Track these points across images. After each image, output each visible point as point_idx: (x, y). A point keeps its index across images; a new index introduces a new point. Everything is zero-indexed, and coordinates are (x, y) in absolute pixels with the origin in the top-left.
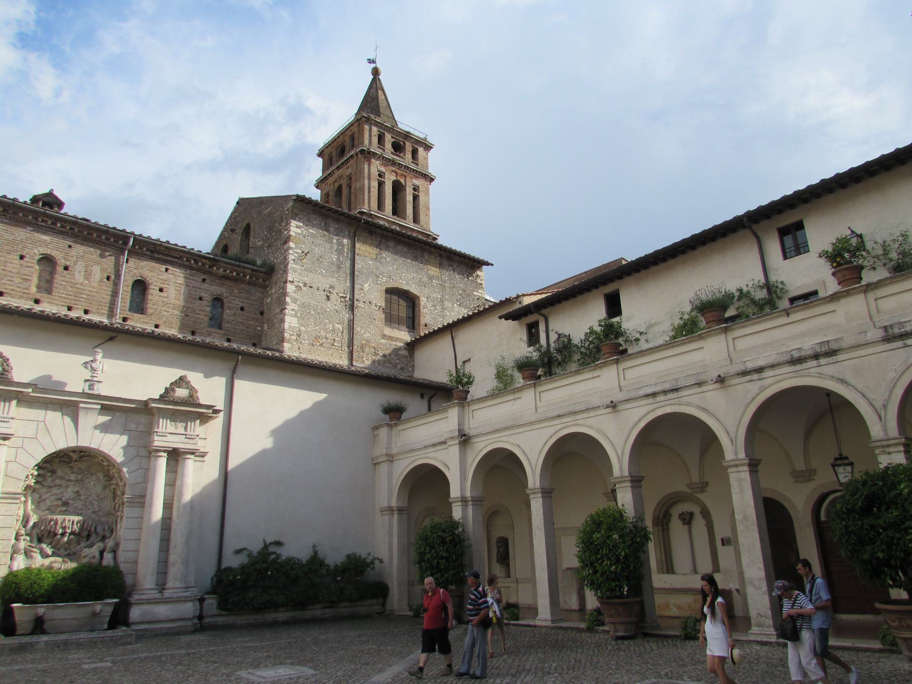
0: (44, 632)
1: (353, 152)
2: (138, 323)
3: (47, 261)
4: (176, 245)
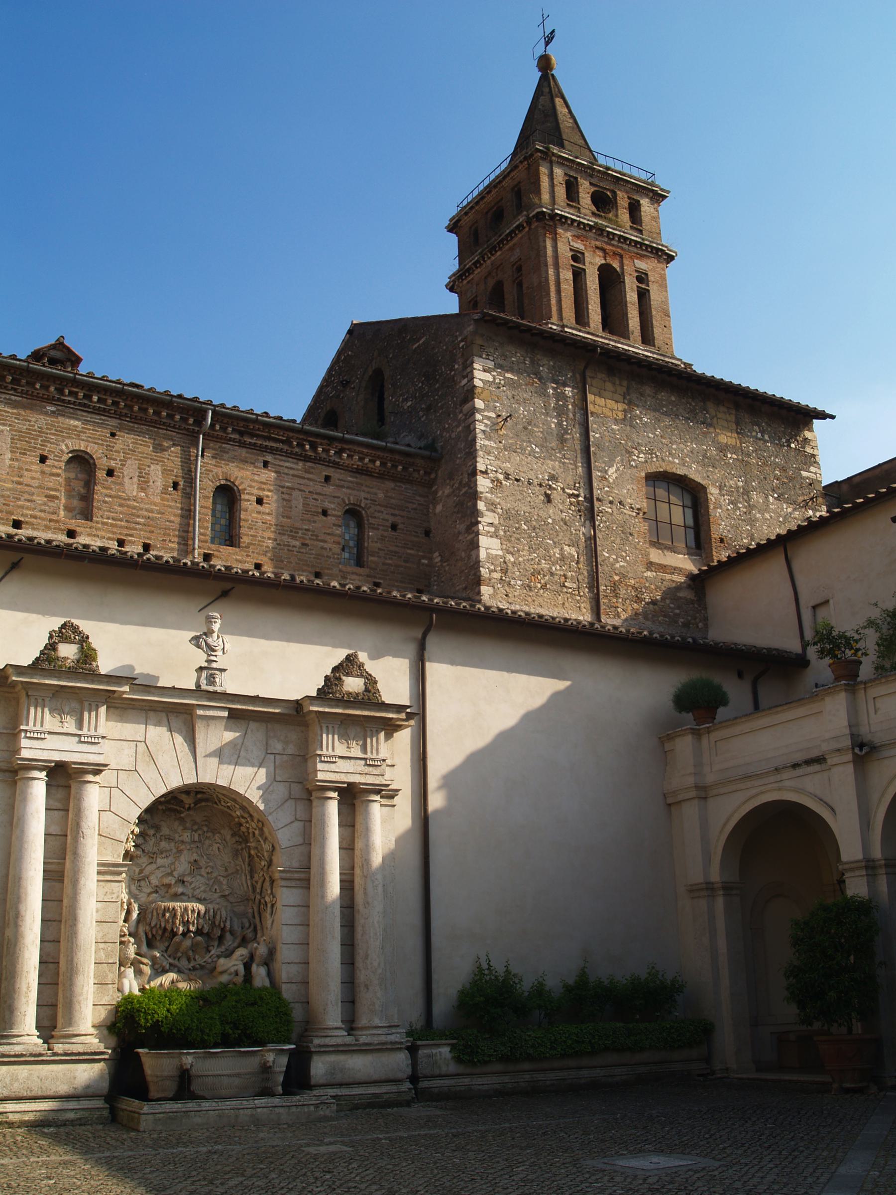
0: (193, 1097)
1: (521, 219)
2: (226, 559)
3: (81, 462)
4: (280, 418)
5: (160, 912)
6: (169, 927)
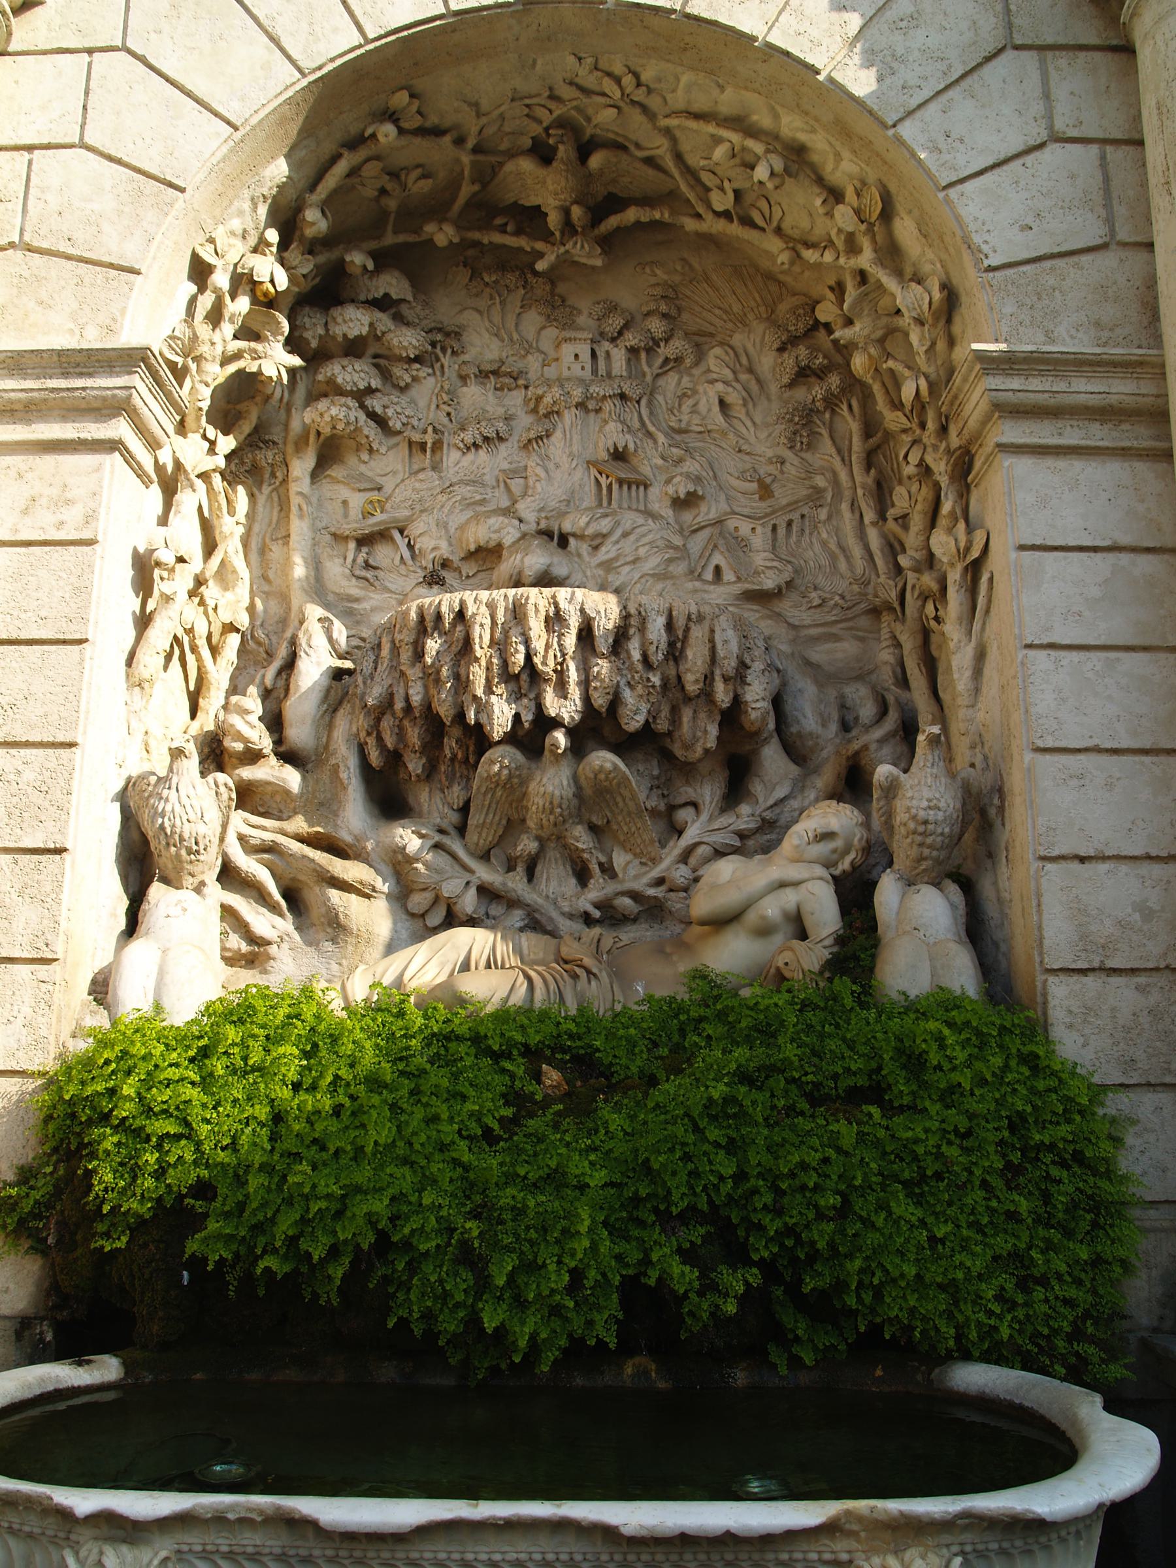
5: (406, 636)
6: (445, 711)
